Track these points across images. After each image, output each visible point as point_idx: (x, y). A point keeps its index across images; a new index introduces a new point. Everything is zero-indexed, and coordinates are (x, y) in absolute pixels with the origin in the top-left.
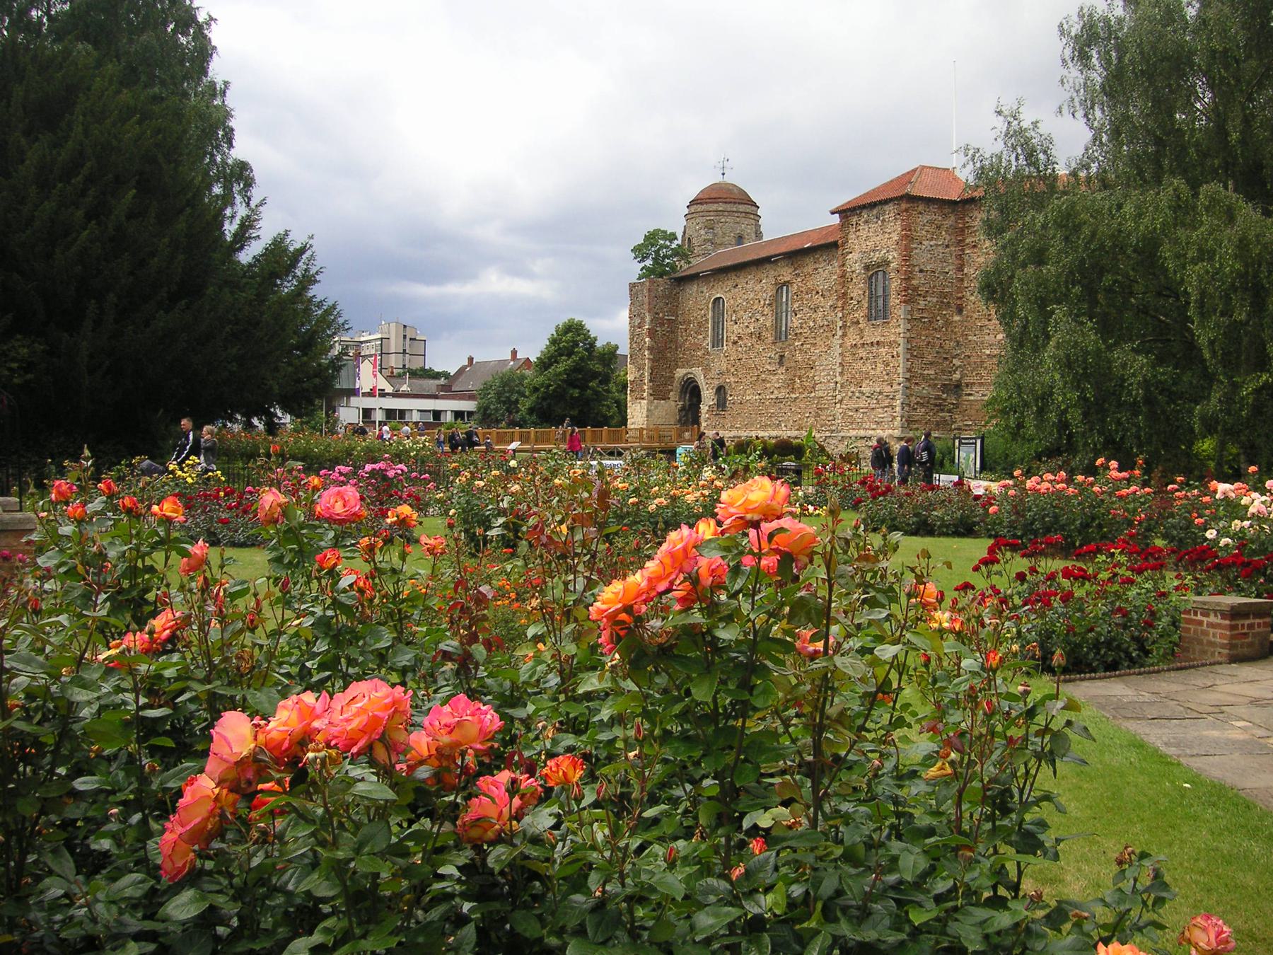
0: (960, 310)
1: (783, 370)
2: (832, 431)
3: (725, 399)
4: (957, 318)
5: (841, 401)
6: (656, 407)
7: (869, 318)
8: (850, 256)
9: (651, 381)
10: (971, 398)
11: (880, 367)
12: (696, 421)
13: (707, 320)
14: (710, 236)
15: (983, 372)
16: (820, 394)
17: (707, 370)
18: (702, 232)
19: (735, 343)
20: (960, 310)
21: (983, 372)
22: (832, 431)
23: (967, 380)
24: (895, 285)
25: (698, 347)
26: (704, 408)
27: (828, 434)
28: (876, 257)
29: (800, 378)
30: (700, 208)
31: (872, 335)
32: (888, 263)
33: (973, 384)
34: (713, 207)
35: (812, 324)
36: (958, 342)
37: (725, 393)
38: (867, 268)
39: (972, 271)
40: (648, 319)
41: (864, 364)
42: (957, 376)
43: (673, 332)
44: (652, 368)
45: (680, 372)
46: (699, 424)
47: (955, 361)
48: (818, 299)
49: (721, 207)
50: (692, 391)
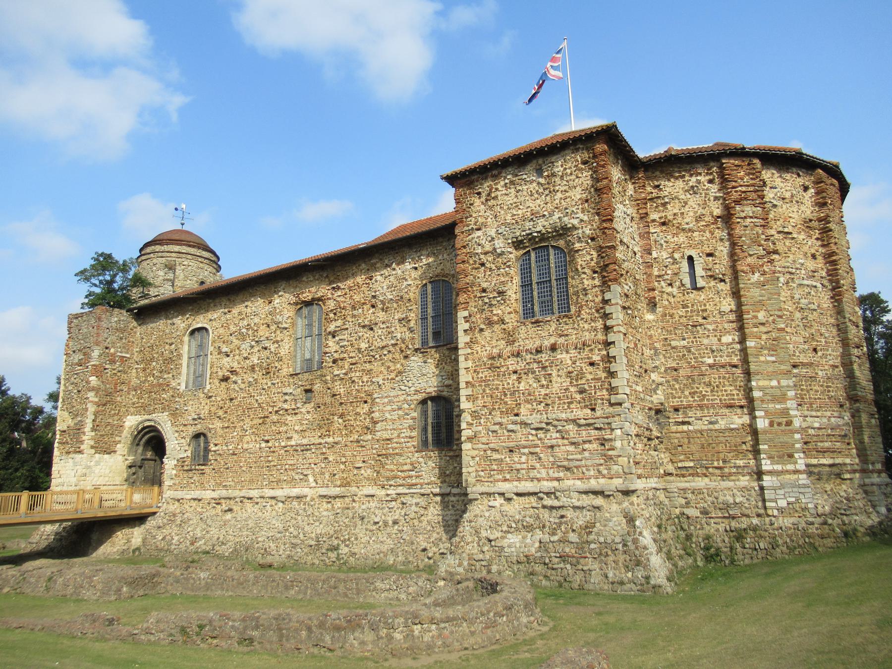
0: (652, 305)
1: (309, 407)
2: (411, 486)
3: (207, 450)
4: (649, 317)
5: (470, 439)
6: (98, 463)
7: (528, 313)
8: (479, 233)
9: (93, 429)
10: (685, 428)
11: (559, 383)
12: (156, 480)
13: (180, 356)
14: (171, 276)
15: (703, 389)
16: (386, 435)
17: (175, 414)
18: (161, 273)
19: (225, 379)
20: (652, 305)
21: (703, 389)
22: (411, 486)
23: (676, 402)
24: (586, 258)
25: (164, 387)
26: (169, 463)
27: (401, 490)
28: (541, 225)
29: (342, 416)
30: (158, 248)
31: (529, 337)
32: (563, 231)
33: (690, 407)
34: (177, 248)
35: (363, 346)
36: (656, 349)
37: (207, 442)
38: (518, 244)
39: (665, 255)
40: (96, 353)
41: (519, 379)
42: (658, 397)
43: (125, 372)
44: (96, 414)
45: (132, 422)
46: (160, 484)
47: (654, 376)
48: (369, 315)
49: (184, 249)
50: (153, 442)
